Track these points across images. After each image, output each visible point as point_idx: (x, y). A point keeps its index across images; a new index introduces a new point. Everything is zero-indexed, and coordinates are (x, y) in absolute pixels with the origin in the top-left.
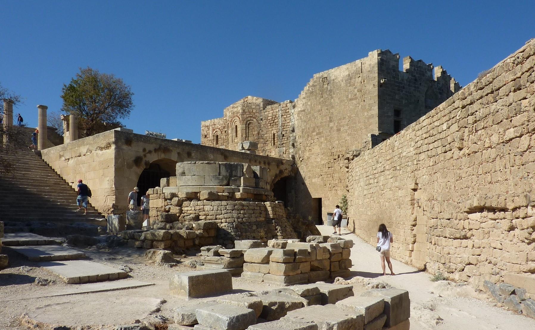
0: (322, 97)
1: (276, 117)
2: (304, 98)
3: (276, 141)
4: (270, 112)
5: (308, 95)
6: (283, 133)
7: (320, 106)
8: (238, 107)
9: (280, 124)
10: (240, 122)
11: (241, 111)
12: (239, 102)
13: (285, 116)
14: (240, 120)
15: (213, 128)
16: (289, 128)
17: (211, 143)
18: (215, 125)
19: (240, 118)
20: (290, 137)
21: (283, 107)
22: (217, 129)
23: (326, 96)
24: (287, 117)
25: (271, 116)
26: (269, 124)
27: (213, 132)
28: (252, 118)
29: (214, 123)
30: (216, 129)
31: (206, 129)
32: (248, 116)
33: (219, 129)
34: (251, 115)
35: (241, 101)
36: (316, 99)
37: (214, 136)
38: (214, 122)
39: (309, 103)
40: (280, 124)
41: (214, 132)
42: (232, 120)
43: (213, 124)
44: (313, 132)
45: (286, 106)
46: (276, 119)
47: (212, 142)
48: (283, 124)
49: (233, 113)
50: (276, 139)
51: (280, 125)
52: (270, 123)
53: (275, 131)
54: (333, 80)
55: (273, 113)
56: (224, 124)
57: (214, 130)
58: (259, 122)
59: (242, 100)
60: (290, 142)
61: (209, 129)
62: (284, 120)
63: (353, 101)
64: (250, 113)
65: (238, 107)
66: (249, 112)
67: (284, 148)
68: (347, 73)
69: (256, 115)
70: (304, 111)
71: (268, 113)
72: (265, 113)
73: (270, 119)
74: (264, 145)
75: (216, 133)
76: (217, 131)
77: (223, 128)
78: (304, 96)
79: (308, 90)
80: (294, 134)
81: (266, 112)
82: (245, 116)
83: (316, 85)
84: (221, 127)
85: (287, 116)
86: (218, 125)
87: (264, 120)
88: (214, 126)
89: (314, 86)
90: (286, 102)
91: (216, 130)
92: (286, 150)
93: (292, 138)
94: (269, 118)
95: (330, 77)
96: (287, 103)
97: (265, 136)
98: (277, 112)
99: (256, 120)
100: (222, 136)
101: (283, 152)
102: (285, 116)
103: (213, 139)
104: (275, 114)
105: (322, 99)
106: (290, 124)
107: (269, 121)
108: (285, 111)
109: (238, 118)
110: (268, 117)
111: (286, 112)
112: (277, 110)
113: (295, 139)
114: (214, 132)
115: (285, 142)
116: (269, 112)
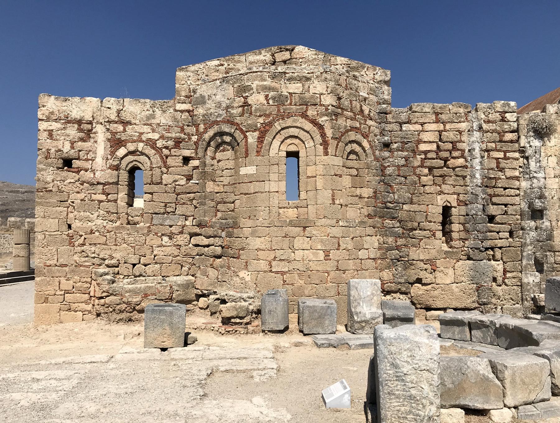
1: (455, 148)
3: (455, 235)
4: (427, 127)
6: (492, 210)
8: (308, 79)
9: (478, 176)
10: (325, 144)
11: (328, 100)
12: (252, 57)
13: (501, 155)
14: (323, 135)
15: (114, 134)
16: (517, 198)
17: (103, 197)
18: (125, 123)
20: (522, 229)
21: (489, 122)
22: (141, 146)
24: (506, 158)
25: (434, 142)
26: (426, 171)
27: (113, 153)
28: (359, 137)
29: (123, 114)
30: (134, 141)
31: (73, 131)
32: (349, 123)
33: (152, 143)
34: (358, 125)
35: (261, 57)
37: (117, 168)
38: (119, 112)
40: (478, 176)
42: (271, 124)
43: (113, 117)
45: (503, 120)
46: (454, 158)
47: (104, 193)
48: (491, 178)
49: (280, 100)
50: (456, 227)
51: (479, 182)
52: (428, 163)
53: (453, 200)
55: (440, 132)
56: (179, 129)
58: (377, 153)
59: (263, 52)
60: (523, 245)
61: (88, 135)
62: (494, 165)
64: (355, 114)
65: (308, 79)
66: (352, 111)
67: (499, 266)
69: (370, 127)
71: (419, 127)
72: (405, 127)
73: (426, 152)
74: (401, 242)
75: (130, 158)
77: (171, 143)
81: (409, 122)
82: (341, 121)
84: (162, 137)
85: (508, 154)
86: (146, 129)
87: (398, 150)
88: (120, 128)
90: (504, 105)
91: (131, 147)
92: (505, 271)
93: (533, 234)
94: (423, 147)
96: (506, 109)
97: (405, 207)
98: (460, 132)
99: (370, 145)
100: (165, 176)
101: (495, 280)
102: (501, 155)
103: (116, 180)
104: (451, 136)
107: (423, 156)
109: (308, 126)
110: (419, 142)
111: (501, 141)
112: (463, 126)
113: (550, 237)
114: (122, 152)
115: (499, 243)
116: (422, 124)
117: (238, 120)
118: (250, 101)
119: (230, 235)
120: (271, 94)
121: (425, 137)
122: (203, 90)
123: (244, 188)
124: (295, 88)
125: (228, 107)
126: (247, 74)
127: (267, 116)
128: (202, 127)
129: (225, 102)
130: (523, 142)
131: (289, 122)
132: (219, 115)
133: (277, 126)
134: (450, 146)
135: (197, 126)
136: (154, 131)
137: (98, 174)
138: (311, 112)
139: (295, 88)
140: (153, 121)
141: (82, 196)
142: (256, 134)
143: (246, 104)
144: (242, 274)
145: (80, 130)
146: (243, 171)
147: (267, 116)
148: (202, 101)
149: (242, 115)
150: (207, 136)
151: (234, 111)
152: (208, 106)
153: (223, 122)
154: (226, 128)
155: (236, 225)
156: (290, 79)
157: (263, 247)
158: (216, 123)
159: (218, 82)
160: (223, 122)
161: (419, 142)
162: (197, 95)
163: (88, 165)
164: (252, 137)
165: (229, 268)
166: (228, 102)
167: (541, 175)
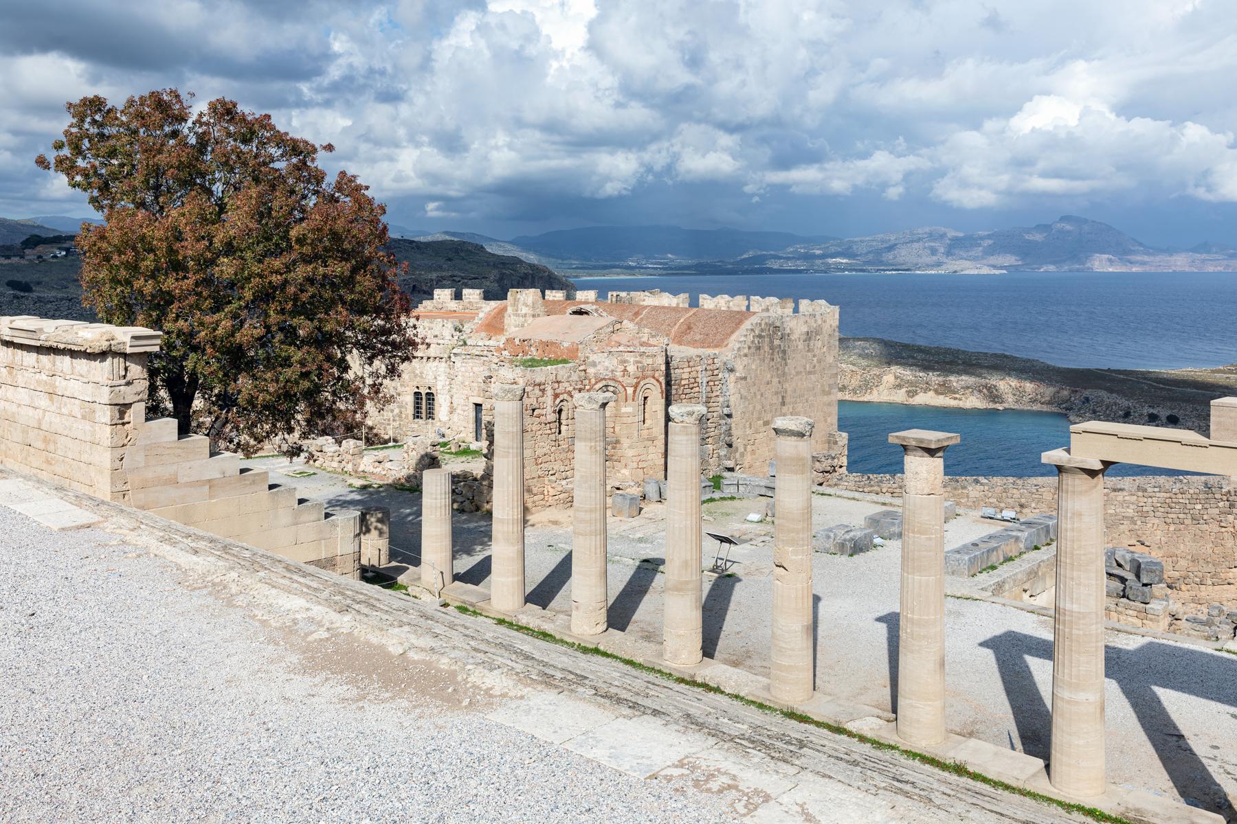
0: (773, 360)
1: (695, 382)
2: (746, 355)
4: (685, 370)
5: (753, 350)
7: (769, 376)
14: (661, 387)
17: (549, 432)
18: (558, 382)
19: (660, 383)
23: (779, 360)
31: (537, 391)
36: (764, 361)
39: (754, 367)
41: (558, 401)
42: (638, 384)
44: (759, 419)
47: (551, 429)
51: (704, 400)
54: (788, 335)
57: (556, 396)
60: (721, 434)
61: (543, 391)
63: (812, 376)
68: (806, 330)
70: (745, 378)
73: (684, 385)
75: (562, 403)
76: (562, 401)
78: (746, 351)
79: (753, 342)
80: (729, 420)
83: (764, 337)
88: (556, 385)
89: (760, 336)
91: (561, 397)
94: (683, 382)
95: (784, 329)
104: (694, 374)
105: (772, 363)
106: (721, 399)
108: (710, 373)
110: (682, 379)
114: (558, 401)
115: (712, 434)
117: (620, 379)
118: (628, 368)
119: (614, 448)
120: (640, 365)
121: (685, 376)
122: (593, 358)
123: (624, 420)
124: (650, 361)
125: (613, 371)
126: (625, 352)
127: (638, 378)
128: (593, 381)
129: (611, 368)
130: (720, 376)
131: (647, 381)
132: (606, 375)
133: (642, 383)
134: (693, 380)
135: (590, 380)
136: (571, 385)
137: (548, 417)
138: (657, 375)
139: (650, 361)
140: (570, 379)
141: (540, 432)
142: (632, 389)
143: (625, 370)
144: (623, 471)
145: (540, 390)
146: (624, 410)
147: (638, 378)
148: (594, 364)
149: (624, 376)
150: (597, 387)
151: (618, 374)
152: (598, 367)
153: (609, 379)
154: (611, 383)
155: (618, 442)
156: (648, 356)
157: (634, 454)
158: (605, 379)
159: (606, 354)
160: (609, 379)
161: (682, 379)
162: (590, 360)
163: (544, 412)
164: (630, 391)
165: (613, 468)
166: (613, 368)
167: (727, 394)
